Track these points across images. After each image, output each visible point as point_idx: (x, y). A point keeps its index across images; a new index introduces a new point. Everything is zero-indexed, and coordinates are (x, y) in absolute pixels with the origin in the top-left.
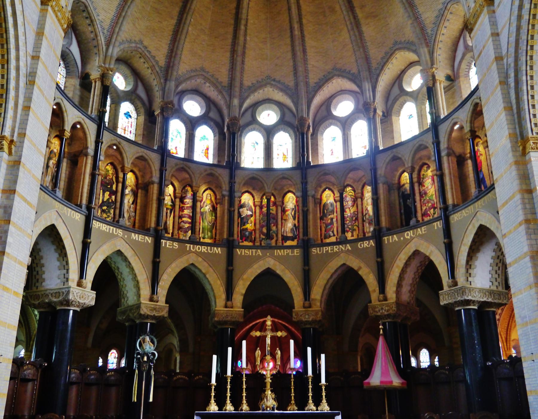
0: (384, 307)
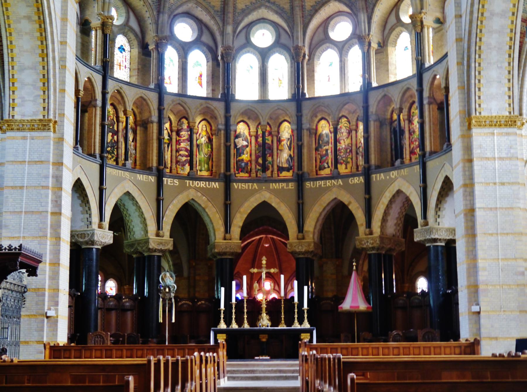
0: (369, 240)
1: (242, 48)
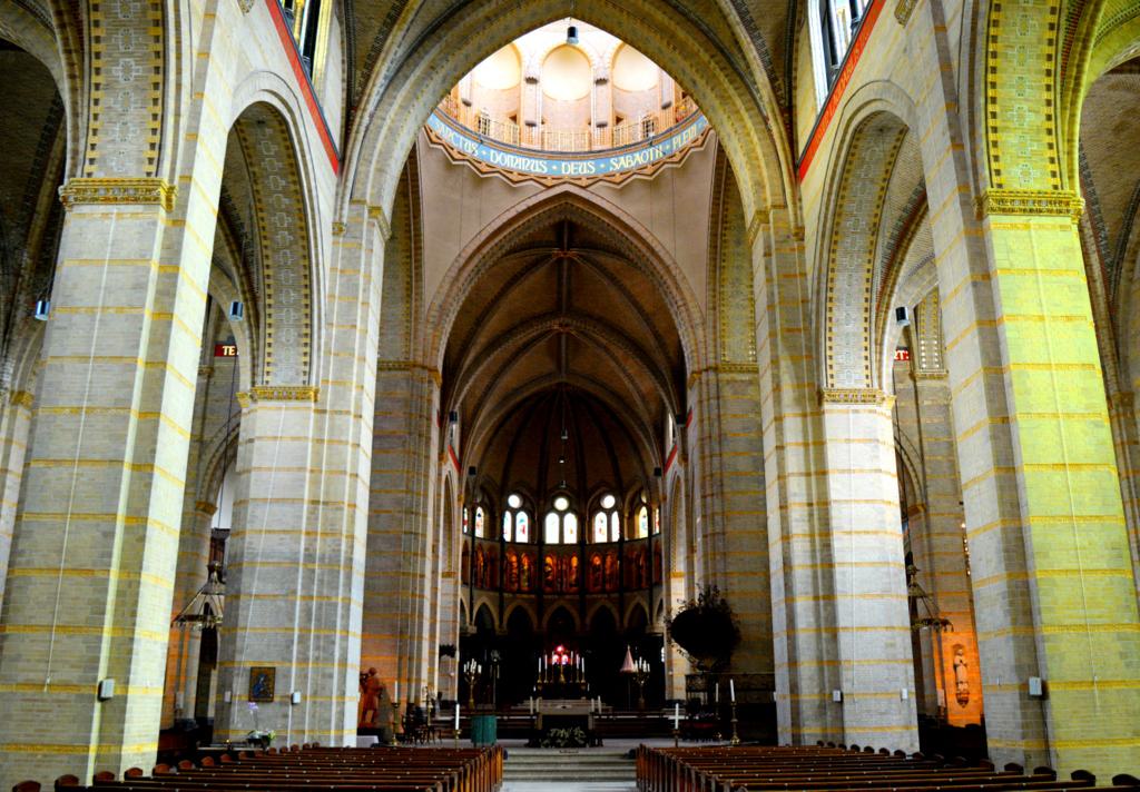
1: (548, 512)
